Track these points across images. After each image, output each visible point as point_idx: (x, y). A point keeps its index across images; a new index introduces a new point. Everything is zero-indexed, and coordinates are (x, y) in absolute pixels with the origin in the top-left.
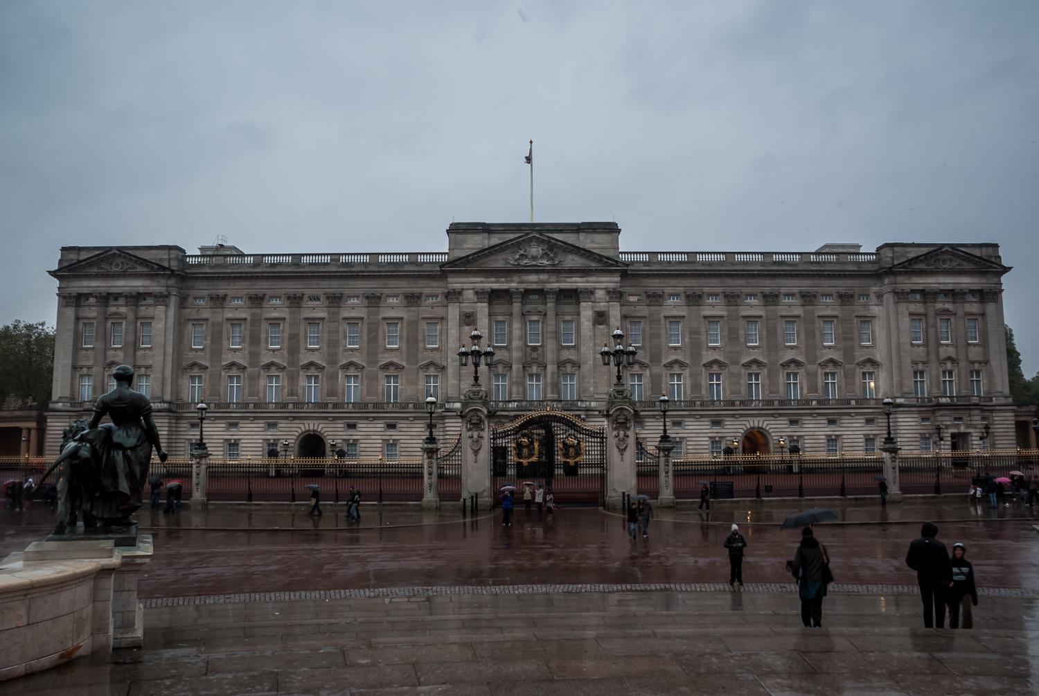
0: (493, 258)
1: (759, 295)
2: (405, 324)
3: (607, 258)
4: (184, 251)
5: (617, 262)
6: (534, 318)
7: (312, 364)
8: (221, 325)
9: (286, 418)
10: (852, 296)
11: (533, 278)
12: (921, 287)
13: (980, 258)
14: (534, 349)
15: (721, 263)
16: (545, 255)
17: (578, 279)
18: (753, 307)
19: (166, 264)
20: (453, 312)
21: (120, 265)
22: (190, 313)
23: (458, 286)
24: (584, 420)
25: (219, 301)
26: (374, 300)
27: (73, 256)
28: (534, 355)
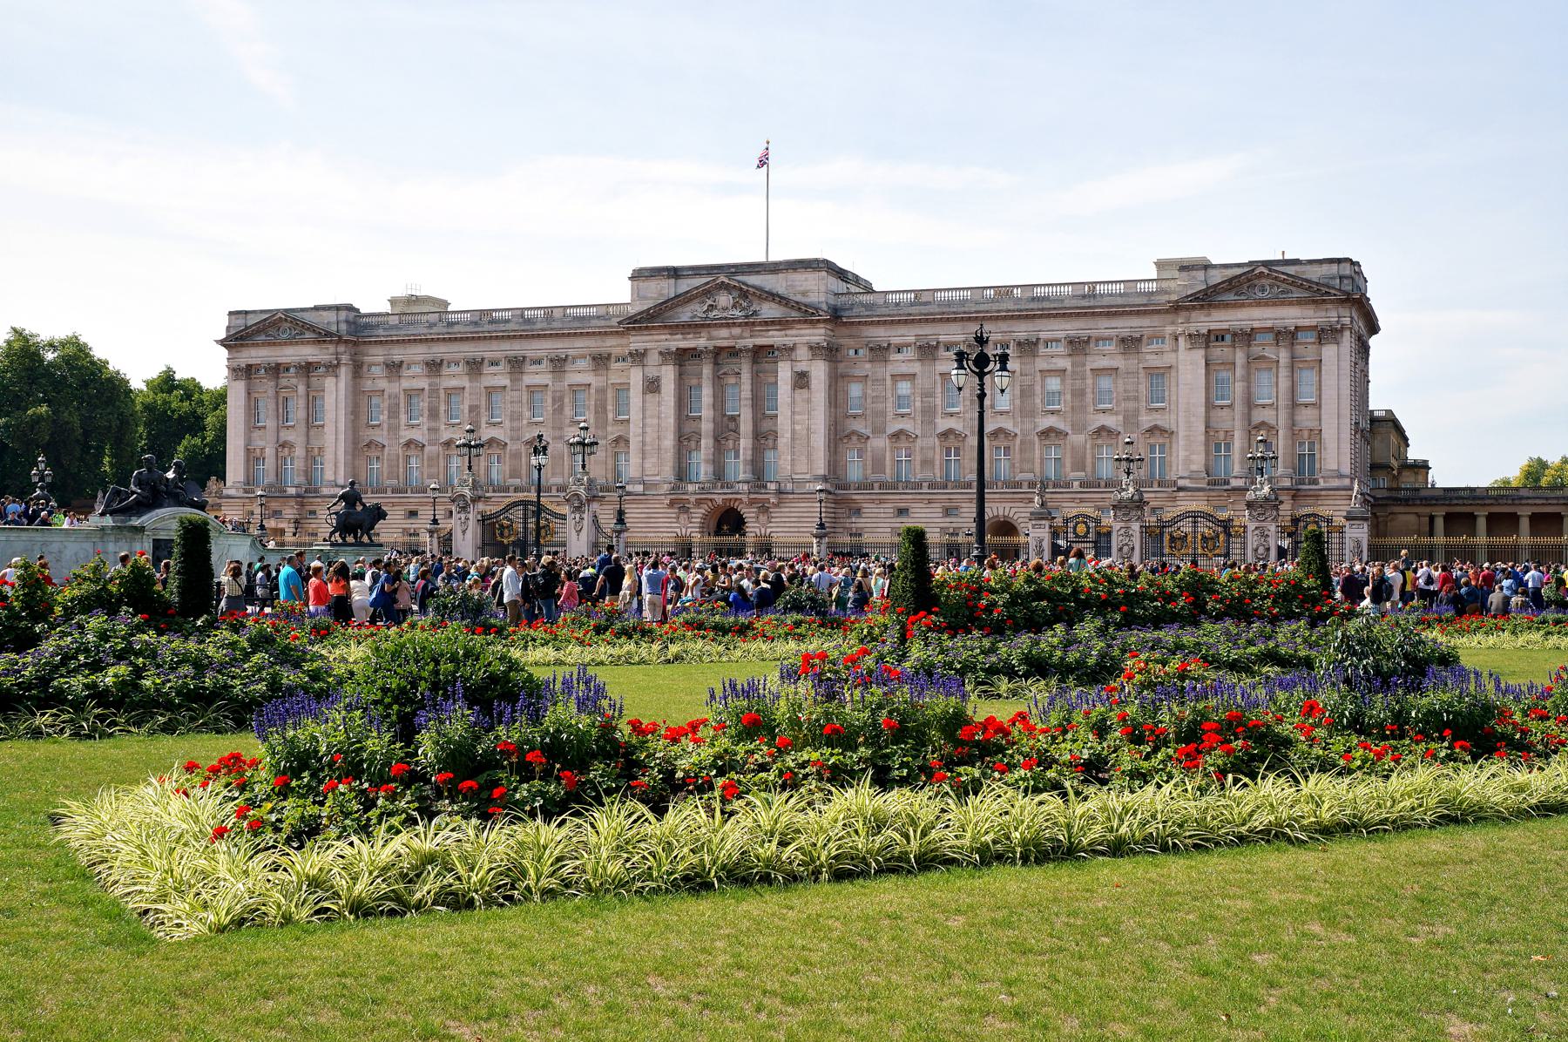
0: (680, 309)
2: (593, 391)
4: (357, 310)
6: (732, 380)
8: (397, 397)
10: (1139, 340)
11: (724, 332)
12: (1225, 326)
14: (734, 419)
15: (963, 302)
19: (334, 328)
20: (636, 377)
22: (368, 385)
24: (777, 505)
27: (240, 322)
28: (732, 425)
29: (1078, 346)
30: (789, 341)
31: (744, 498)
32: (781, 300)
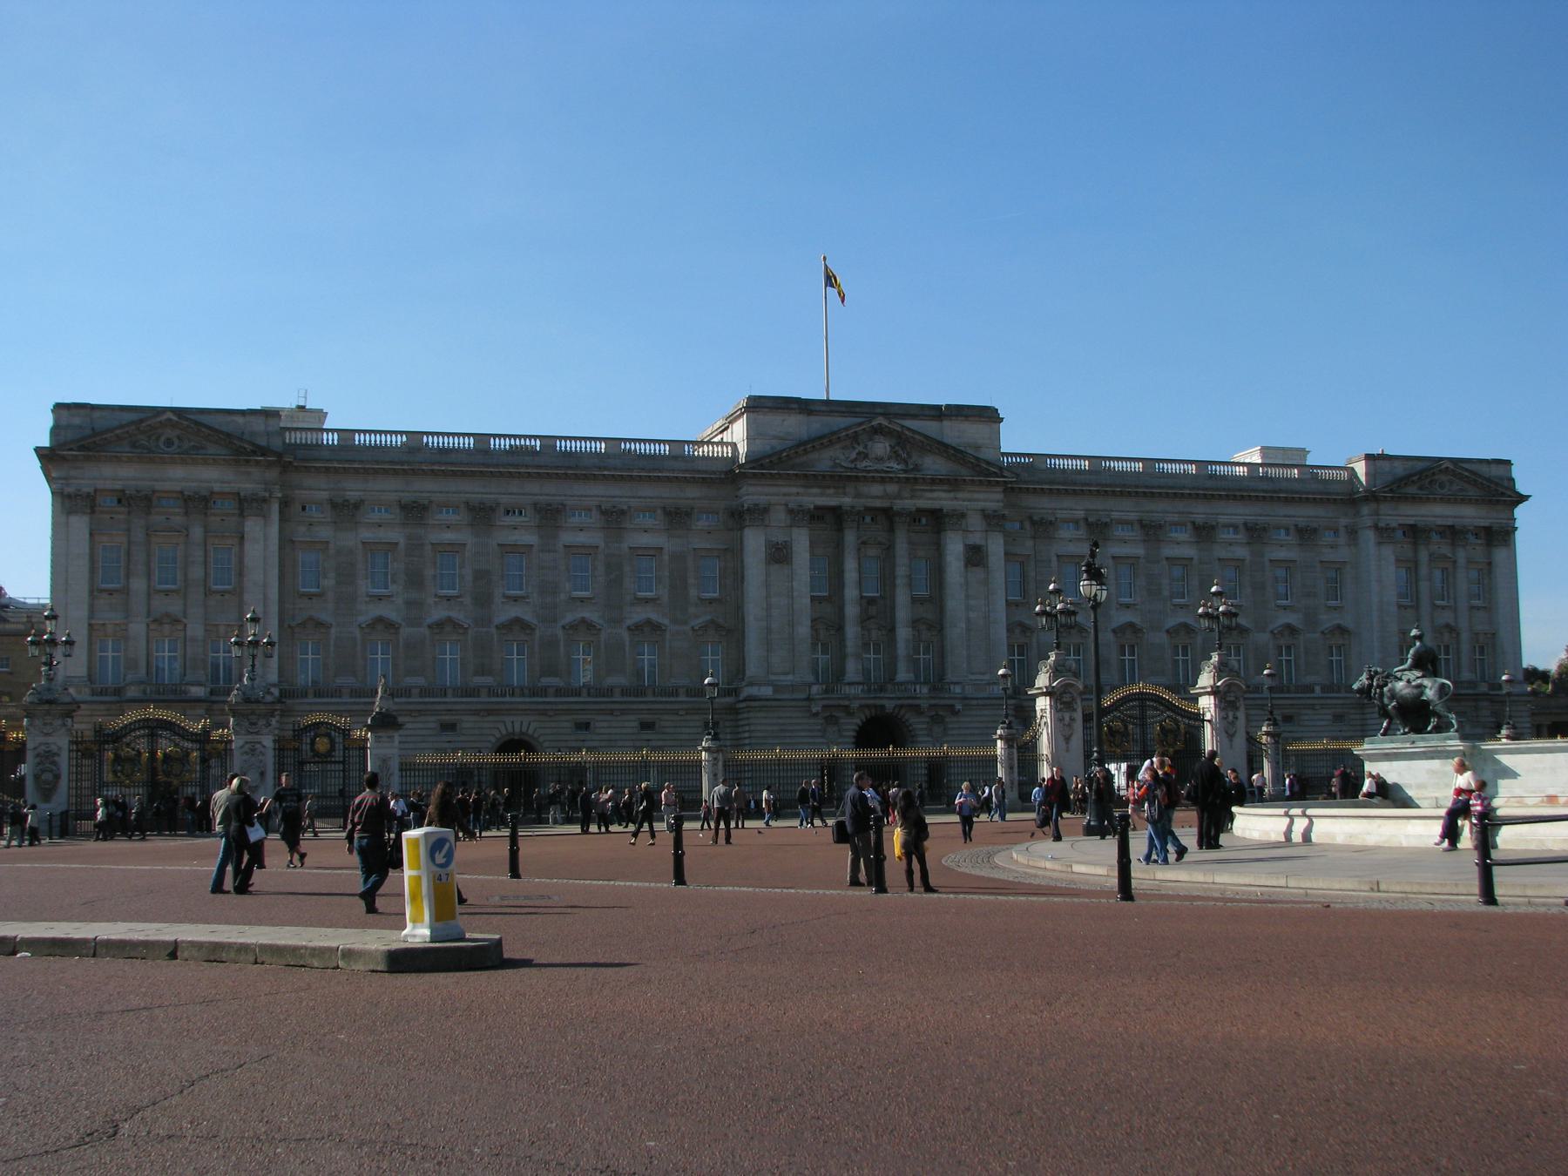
0: (814, 456)
1: (1189, 526)
2: (666, 557)
3: (988, 463)
5: (1001, 468)
6: (872, 551)
7: (517, 621)
9: (476, 713)
10: (1315, 530)
11: (876, 489)
12: (1411, 521)
13: (1489, 480)
14: (871, 601)
16: (895, 456)
17: (943, 495)
18: (1181, 545)
19: (262, 442)
20: (754, 542)
21: (176, 442)
23: (762, 500)
24: (955, 713)
25: (346, 511)
26: (614, 518)
27: (77, 421)
28: (873, 610)
29: (1256, 533)
30: (957, 505)
31: (924, 704)
32: (953, 453)
